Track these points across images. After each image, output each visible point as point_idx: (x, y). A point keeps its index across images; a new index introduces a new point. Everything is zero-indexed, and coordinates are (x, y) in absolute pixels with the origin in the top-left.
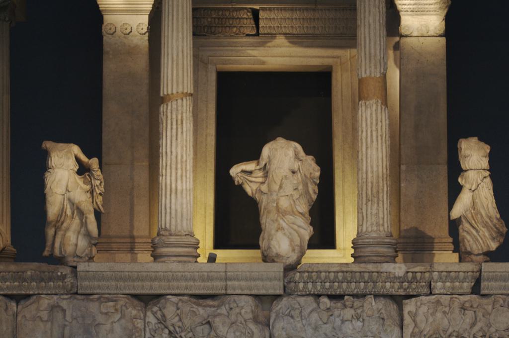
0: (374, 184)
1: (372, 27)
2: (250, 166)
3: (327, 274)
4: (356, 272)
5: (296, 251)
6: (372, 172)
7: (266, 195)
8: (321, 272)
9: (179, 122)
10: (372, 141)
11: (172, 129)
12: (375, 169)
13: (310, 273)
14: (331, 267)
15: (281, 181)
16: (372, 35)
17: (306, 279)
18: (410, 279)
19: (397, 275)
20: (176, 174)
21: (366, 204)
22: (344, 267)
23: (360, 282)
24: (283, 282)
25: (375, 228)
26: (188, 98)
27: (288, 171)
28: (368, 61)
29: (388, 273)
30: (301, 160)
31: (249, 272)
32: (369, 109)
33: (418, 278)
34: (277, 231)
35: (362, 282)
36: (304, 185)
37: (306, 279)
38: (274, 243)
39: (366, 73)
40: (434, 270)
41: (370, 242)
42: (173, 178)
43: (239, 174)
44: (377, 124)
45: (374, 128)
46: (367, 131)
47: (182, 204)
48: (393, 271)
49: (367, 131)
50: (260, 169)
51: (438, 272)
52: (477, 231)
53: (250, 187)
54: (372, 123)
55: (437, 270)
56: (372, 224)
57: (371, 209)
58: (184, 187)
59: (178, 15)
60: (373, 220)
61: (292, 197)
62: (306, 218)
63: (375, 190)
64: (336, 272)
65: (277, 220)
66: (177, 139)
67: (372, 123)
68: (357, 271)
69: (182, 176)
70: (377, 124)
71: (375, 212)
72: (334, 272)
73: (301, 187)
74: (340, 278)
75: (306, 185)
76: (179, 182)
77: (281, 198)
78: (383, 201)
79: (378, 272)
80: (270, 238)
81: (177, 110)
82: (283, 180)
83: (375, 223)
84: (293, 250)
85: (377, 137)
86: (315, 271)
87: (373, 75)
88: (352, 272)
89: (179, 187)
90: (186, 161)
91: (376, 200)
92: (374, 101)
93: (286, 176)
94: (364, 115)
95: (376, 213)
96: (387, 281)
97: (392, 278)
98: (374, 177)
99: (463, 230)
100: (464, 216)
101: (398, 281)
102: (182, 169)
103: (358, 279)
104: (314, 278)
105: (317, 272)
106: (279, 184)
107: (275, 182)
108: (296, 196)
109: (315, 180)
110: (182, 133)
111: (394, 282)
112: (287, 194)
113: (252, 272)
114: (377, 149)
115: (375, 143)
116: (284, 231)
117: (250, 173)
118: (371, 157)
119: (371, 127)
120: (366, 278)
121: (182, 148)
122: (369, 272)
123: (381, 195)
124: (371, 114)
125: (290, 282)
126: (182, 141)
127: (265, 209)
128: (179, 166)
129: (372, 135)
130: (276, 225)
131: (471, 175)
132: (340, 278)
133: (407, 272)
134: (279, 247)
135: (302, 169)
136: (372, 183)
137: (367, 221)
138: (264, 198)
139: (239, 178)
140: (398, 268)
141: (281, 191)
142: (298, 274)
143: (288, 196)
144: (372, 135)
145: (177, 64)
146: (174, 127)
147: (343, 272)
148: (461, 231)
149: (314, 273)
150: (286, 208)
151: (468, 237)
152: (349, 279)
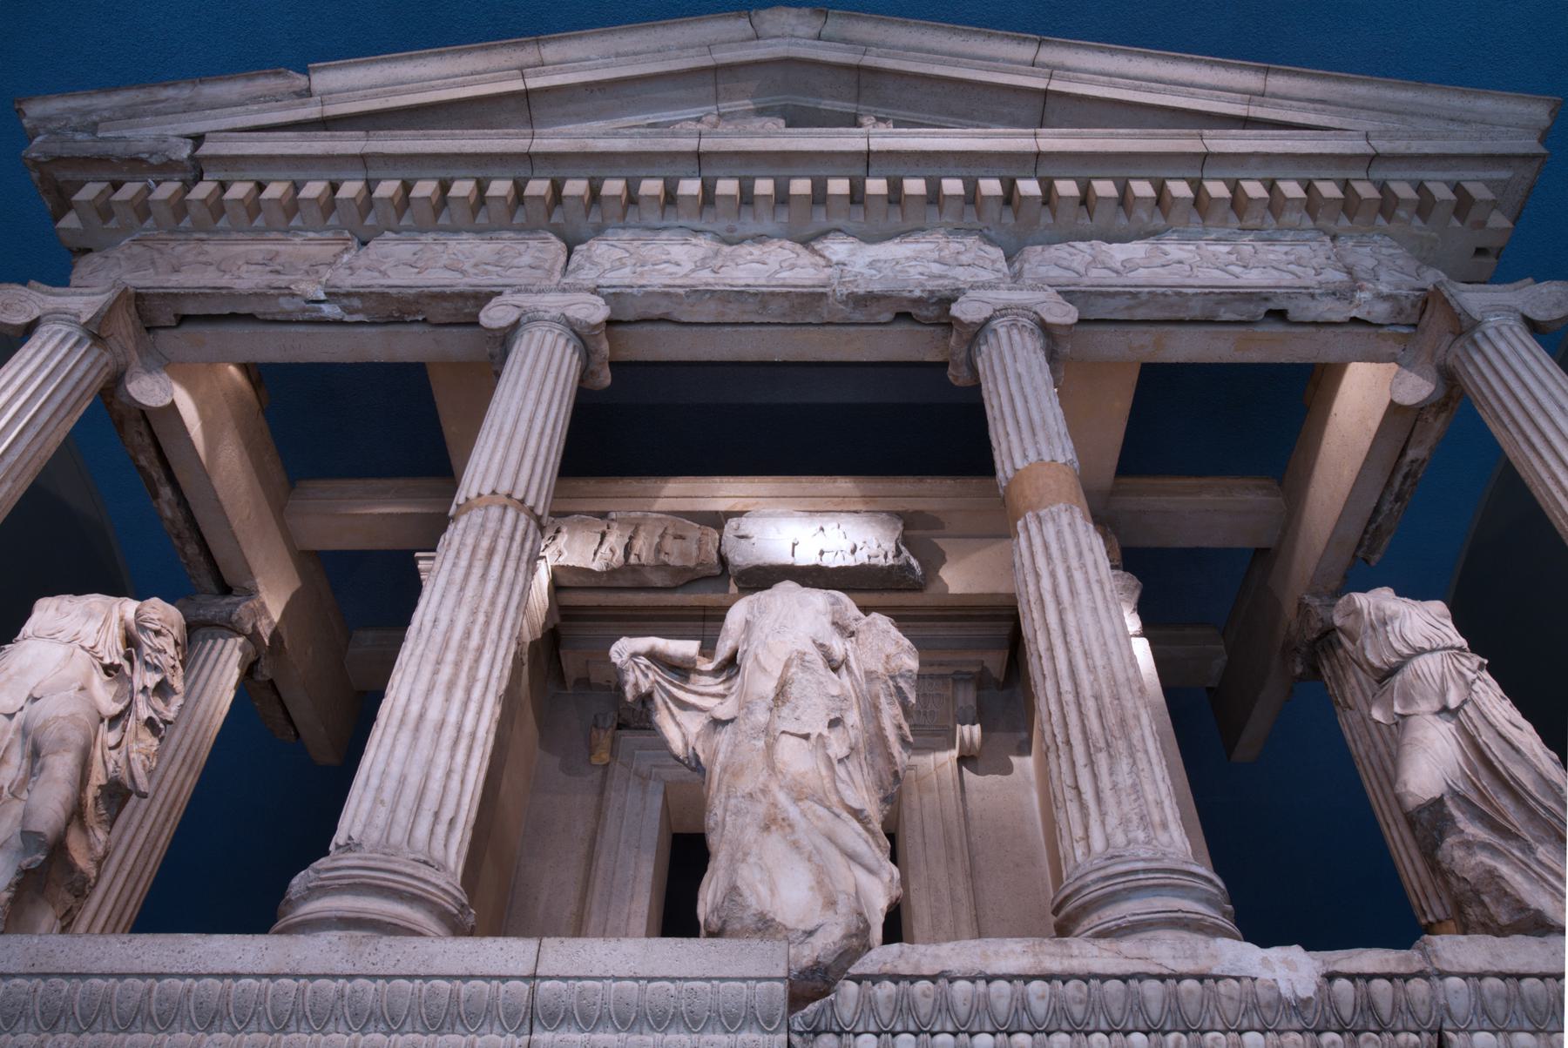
0: (1107, 700)
1: (1026, 380)
2: (686, 648)
3: (981, 984)
4: (1104, 978)
5: (842, 908)
6: (1092, 669)
7: (729, 727)
8: (952, 980)
9: (481, 553)
10: (1073, 592)
11: (454, 565)
12: (1099, 661)
13: (904, 984)
14: (996, 953)
15: (787, 666)
16: (1028, 390)
17: (885, 1015)
18: (1346, 1012)
19: (1286, 991)
20: (436, 672)
21: (1091, 763)
22: (1052, 955)
23: (1127, 1033)
24: (783, 1037)
25: (1141, 835)
26: (523, 516)
27: (810, 642)
28: (1026, 434)
29: (1246, 982)
30: (852, 634)
31: (636, 979)
32: (1050, 529)
33: (1385, 1008)
34: (767, 828)
35: (1136, 1030)
36: (863, 715)
37: (885, 1015)
38: (748, 875)
39: (1025, 456)
40: (1446, 967)
41: (1136, 872)
42: (422, 686)
43: (643, 661)
44: (1080, 554)
45: (1074, 563)
46: (1053, 575)
47: (430, 762)
48: (1265, 975)
49: (1053, 575)
50: (716, 672)
51: (1465, 976)
52: (1528, 849)
53: (678, 725)
54: (1064, 551)
55: (1456, 969)
56: (1124, 822)
57: (1111, 775)
58: (452, 718)
59: (536, 361)
60: (1126, 808)
61: (825, 746)
62: (868, 830)
63: (1111, 719)
64: (1019, 977)
65: (765, 791)
66: (462, 589)
67: (1064, 551)
68: (1111, 970)
69: (451, 685)
70: (1080, 554)
71: (1129, 782)
72: (1010, 978)
73: (853, 718)
74: (1039, 1008)
75: (872, 711)
76: (437, 699)
77: (784, 737)
78: (1146, 752)
79: (1200, 978)
80: (739, 855)
81: (483, 525)
82: (793, 670)
83: (1135, 819)
84: (831, 903)
85: (1088, 582)
86: (926, 972)
87: (1047, 459)
88: (1086, 978)
89: (433, 714)
90: (480, 650)
91: (1121, 745)
92: (1062, 506)
93: (802, 655)
94: (1037, 541)
95: (1134, 785)
96: (1245, 1024)
97: (1269, 1006)
98: (1102, 680)
99: (1468, 845)
100: (1456, 795)
101: (1296, 1024)
102: (457, 664)
103: (1117, 1015)
104: (925, 1008)
105: (933, 979)
106: (777, 674)
107: (764, 670)
108: (837, 748)
109: (902, 684)
110: (484, 576)
111: (1279, 1033)
112: (805, 731)
113: (651, 979)
114: (1095, 609)
115: (1084, 597)
116: (793, 832)
117: (680, 670)
118: (1079, 632)
119: (1065, 559)
120: (1155, 1009)
121: (474, 612)
122: (1162, 978)
123: (1136, 735)
124: (1059, 533)
125: (817, 1033)
126: (479, 596)
127: (724, 770)
128: (450, 656)
129: (1070, 578)
130: (761, 809)
131: (1429, 665)
132: (1039, 1008)
133: (1330, 977)
134: (773, 892)
135: (857, 659)
136: (1097, 697)
137: (1103, 814)
138: (724, 737)
139: (638, 673)
140: (1291, 970)
141: (785, 711)
142: (851, 988)
143: (806, 737)
144: (1070, 578)
145: (511, 438)
146: (463, 563)
147: (1048, 978)
148: (1458, 854)
149: (923, 985)
150: (803, 775)
151: (1504, 869)
152: (1078, 1011)
